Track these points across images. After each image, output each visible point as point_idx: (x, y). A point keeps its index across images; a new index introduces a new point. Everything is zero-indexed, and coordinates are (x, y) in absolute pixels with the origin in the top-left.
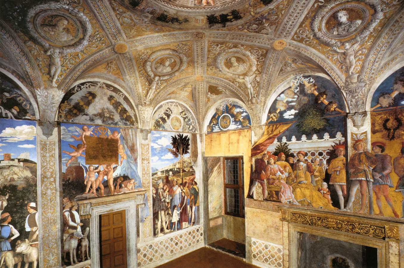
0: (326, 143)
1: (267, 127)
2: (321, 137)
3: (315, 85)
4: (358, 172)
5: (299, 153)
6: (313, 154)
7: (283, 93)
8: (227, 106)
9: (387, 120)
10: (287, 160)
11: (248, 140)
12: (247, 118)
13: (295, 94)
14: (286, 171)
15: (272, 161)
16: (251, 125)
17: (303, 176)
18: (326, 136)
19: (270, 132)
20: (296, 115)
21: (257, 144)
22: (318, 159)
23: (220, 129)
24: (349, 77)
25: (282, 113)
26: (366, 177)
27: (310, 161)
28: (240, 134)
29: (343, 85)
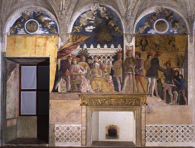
0: (112, 50)
1: (72, 36)
2: (109, 47)
3: (106, 13)
4: (129, 68)
5: (95, 56)
6: (104, 58)
7: (85, 12)
8: (34, 13)
9: (142, 40)
10: (87, 61)
11: (55, 45)
12: (54, 27)
13: (94, 15)
14: (85, 69)
15: (75, 62)
16: (58, 32)
17: (97, 72)
18: (112, 46)
19: (75, 40)
21: (64, 48)
22: (107, 61)
23: (26, 32)
24: (127, 11)
25: (84, 27)
26: (132, 72)
27: (102, 62)
28: (47, 39)
29: (124, 15)
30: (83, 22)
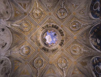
7: (92, 43)
20: (99, 39)
24: (89, 25)
25: (98, 44)
30: (96, 44)
